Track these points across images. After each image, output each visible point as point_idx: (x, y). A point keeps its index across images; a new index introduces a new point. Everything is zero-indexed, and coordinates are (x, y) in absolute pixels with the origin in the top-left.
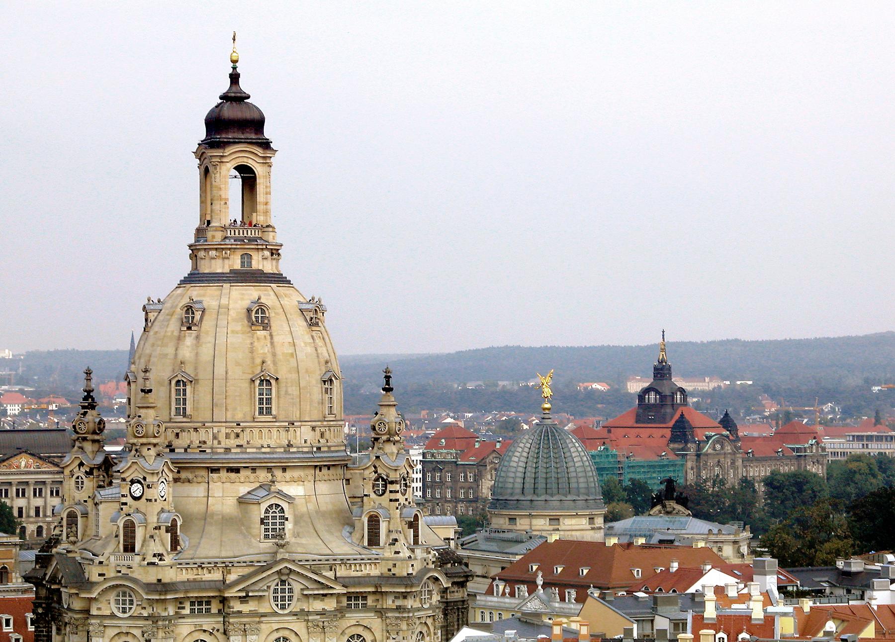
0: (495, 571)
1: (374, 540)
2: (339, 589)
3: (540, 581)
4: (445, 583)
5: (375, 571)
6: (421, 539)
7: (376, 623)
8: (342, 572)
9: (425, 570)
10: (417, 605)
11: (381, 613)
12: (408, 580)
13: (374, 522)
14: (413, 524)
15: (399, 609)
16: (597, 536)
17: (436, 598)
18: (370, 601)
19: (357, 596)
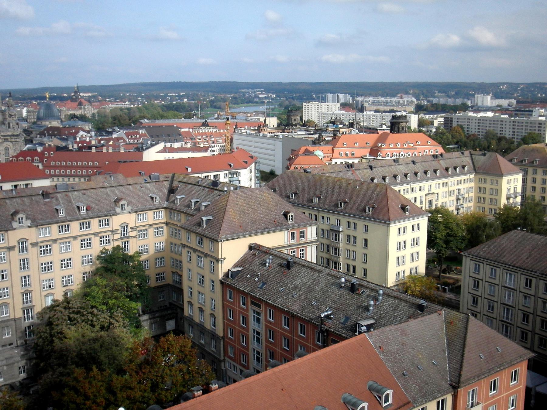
0: (38, 133)
1: (9, 127)
2: (2, 137)
3: (47, 135)
4: (25, 136)
5: (9, 133)
6: (19, 127)
7: (11, 144)
8: (2, 134)
9: (20, 133)
10: (19, 140)
11: (12, 142)
12: (17, 135)
13: (9, 124)
14: (18, 124)
15: (15, 141)
16: (58, 125)
17: (23, 139)
18: (9, 140)
19: (6, 139)
